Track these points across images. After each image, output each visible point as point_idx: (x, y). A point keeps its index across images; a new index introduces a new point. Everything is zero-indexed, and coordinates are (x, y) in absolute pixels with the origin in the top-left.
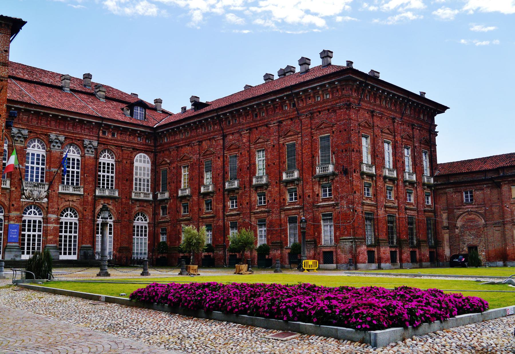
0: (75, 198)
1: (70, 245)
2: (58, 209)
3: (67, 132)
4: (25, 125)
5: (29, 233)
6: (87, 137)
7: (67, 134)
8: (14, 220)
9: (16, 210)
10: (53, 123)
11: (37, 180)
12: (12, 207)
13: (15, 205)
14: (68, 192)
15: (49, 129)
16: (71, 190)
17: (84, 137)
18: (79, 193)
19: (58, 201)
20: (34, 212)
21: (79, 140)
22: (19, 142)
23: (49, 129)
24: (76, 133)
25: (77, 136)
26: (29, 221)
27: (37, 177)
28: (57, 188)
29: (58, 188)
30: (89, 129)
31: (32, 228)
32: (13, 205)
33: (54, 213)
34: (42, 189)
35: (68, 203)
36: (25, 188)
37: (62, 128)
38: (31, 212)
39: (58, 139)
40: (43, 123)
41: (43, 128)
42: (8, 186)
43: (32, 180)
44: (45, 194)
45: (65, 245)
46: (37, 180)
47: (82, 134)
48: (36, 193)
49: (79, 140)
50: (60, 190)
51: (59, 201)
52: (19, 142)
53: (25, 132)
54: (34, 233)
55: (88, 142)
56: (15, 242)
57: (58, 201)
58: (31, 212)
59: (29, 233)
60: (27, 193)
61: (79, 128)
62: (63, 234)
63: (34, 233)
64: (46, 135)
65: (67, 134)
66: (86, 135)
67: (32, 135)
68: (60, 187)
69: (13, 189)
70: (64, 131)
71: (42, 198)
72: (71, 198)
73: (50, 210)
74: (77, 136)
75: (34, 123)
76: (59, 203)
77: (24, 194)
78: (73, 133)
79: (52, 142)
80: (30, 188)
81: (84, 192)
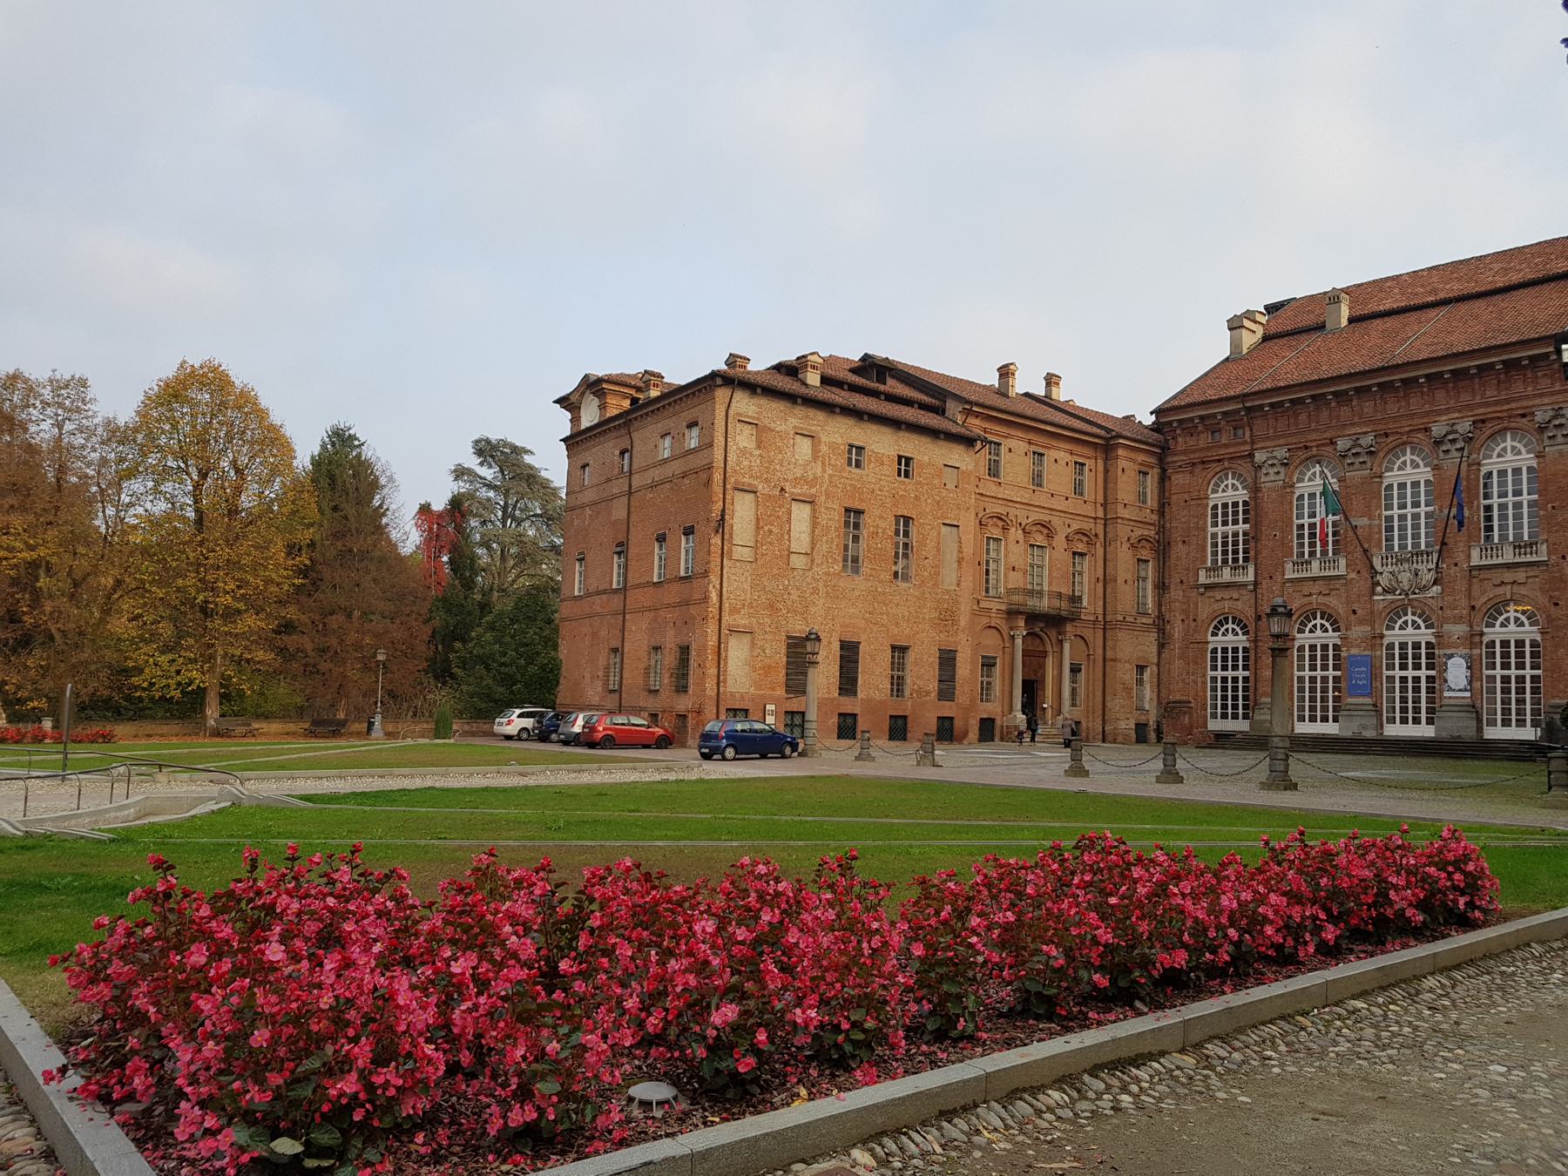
0: (1521, 575)
1: (1313, 699)
2: (1473, 608)
3: (1481, 405)
4: (1366, 423)
5: (1404, 673)
6: (1546, 401)
7: (1481, 411)
8: (1358, 646)
9: (1361, 622)
10: (1440, 395)
11: (1416, 545)
12: (1353, 617)
13: (1359, 612)
14: (1500, 561)
15: (1427, 414)
16: (1508, 556)
17: (1537, 402)
18: (1534, 558)
19: (1469, 590)
20: (1414, 622)
21: (1523, 416)
22: (1357, 466)
23: (1427, 414)
24: (1508, 401)
25: (1513, 405)
26: (1403, 646)
27: (1416, 536)
28: (1462, 556)
29: (1469, 556)
30: (1551, 377)
31: (1410, 661)
32: (1354, 612)
33: (1458, 620)
34: (1420, 566)
35: (1500, 590)
36: (1378, 568)
37: (1465, 397)
38: (1406, 622)
39: (1456, 432)
40: (1416, 404)
41: (1412, 416)
42: (1342, 571)
43: (1403, 547)
44: (1430, 576)
45: (1235, 698)
46: (1416, 545)
47: (1527, 397)
48: (1405, 577)
49: (1523, 416)
50: (1475, 561)
51: (1475, 587)
52: (1357, 466)
53: (1368, 440)
54: (1417, 673)
55: (1551, 413)
56: (1363, 695)
57: (1469, 590)
58: (1406, 622)
59: (1404, 673)
60: (1384, 580)
61: (1520, 383)
62: (1331, 673)
63: (1417, 673)
64: (1426, 430)
65: (1481, 411)
66: (1541, 395)
67: (1391, 439)
68: (1475, 553)
69: (1353, 575)
70: (1470, 407)
71: (1424, 588)
72: (1508, 576)
73: (1448, 613)
74: (1513, 405)
75: (1393, 408)
76: (1476, 593)
77: (1378, 584)
78: (1497, 403)
79: (1438, 443)
80: (1390, 568)
81: (1549, 553)
